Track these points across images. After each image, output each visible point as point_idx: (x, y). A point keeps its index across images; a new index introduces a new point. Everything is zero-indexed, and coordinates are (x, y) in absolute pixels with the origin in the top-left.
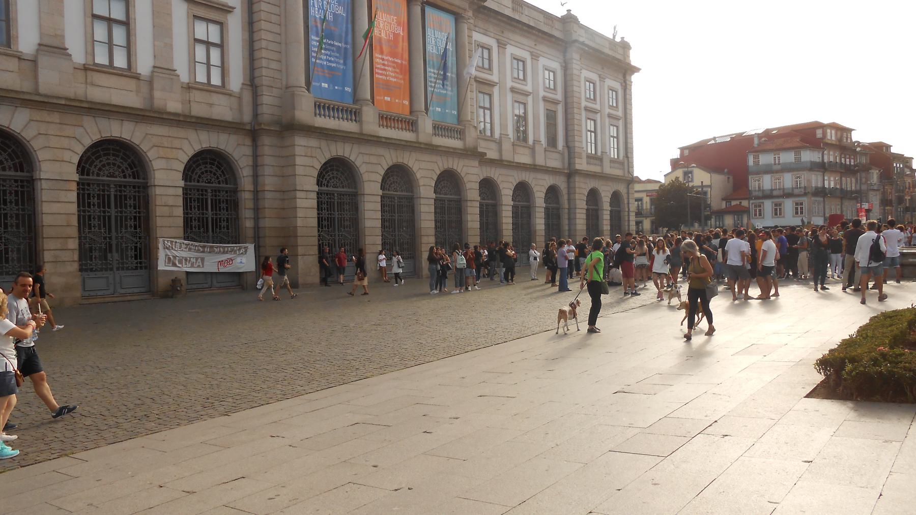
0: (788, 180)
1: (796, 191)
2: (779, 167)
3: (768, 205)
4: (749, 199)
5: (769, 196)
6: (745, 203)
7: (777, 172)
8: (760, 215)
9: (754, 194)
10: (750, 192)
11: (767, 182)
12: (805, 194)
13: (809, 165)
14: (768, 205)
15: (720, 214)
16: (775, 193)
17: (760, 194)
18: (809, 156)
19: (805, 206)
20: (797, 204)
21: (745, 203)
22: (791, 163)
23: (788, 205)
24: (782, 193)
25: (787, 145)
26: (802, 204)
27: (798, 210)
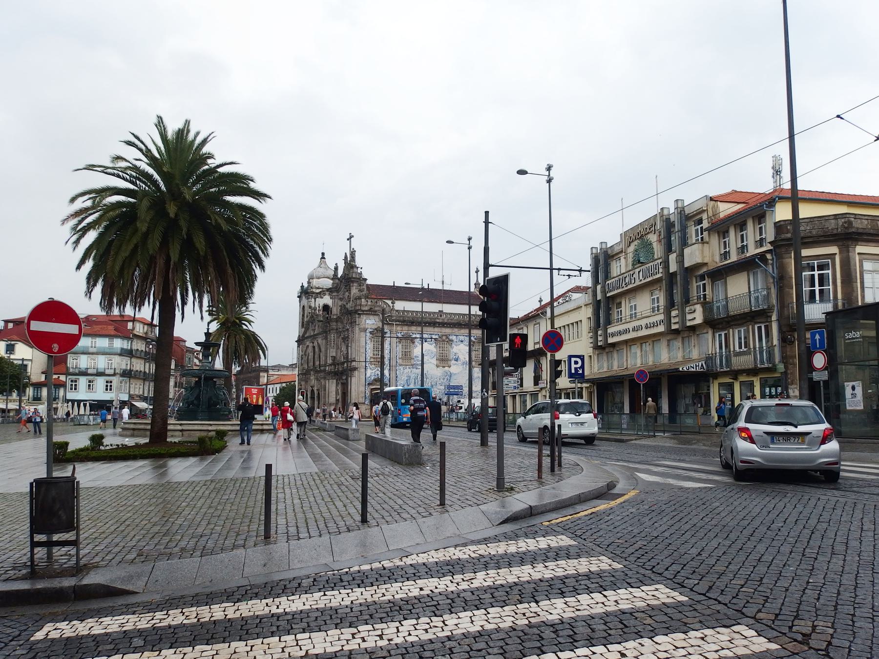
0: (102, 363)
1: (107, 372)
2: (94, 350)
3: (83, 381)
4: (67, 373)
5: (84, 373)
6: (63, 378)
7: (93, 354)
8: (75, 389)
9: (71, 370)
10: (67, 368)
11: (83, 362)
12: (114, 375)
13: (119, 351)
14: (83, 381)
15: (38, 386)
16: (90, 371)
17: (77, 371)
18: (119, 344)
19: (114, 384)
20: (107, 382)
21: (63, 378)
22: (104, 348)
23: (100, 382)
24: (95, 371)
25: (104, 333)
26: (111, 382)
27: (108, 387)
